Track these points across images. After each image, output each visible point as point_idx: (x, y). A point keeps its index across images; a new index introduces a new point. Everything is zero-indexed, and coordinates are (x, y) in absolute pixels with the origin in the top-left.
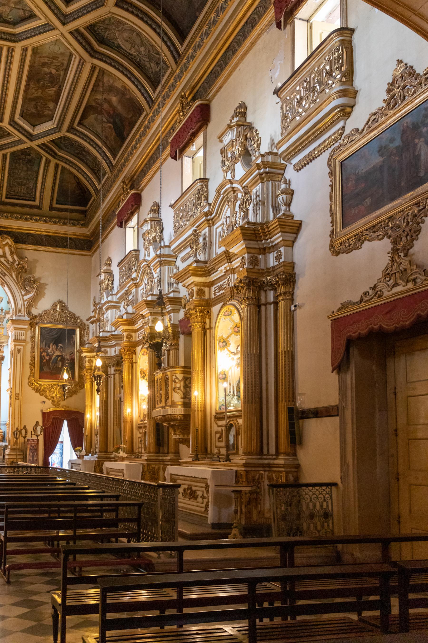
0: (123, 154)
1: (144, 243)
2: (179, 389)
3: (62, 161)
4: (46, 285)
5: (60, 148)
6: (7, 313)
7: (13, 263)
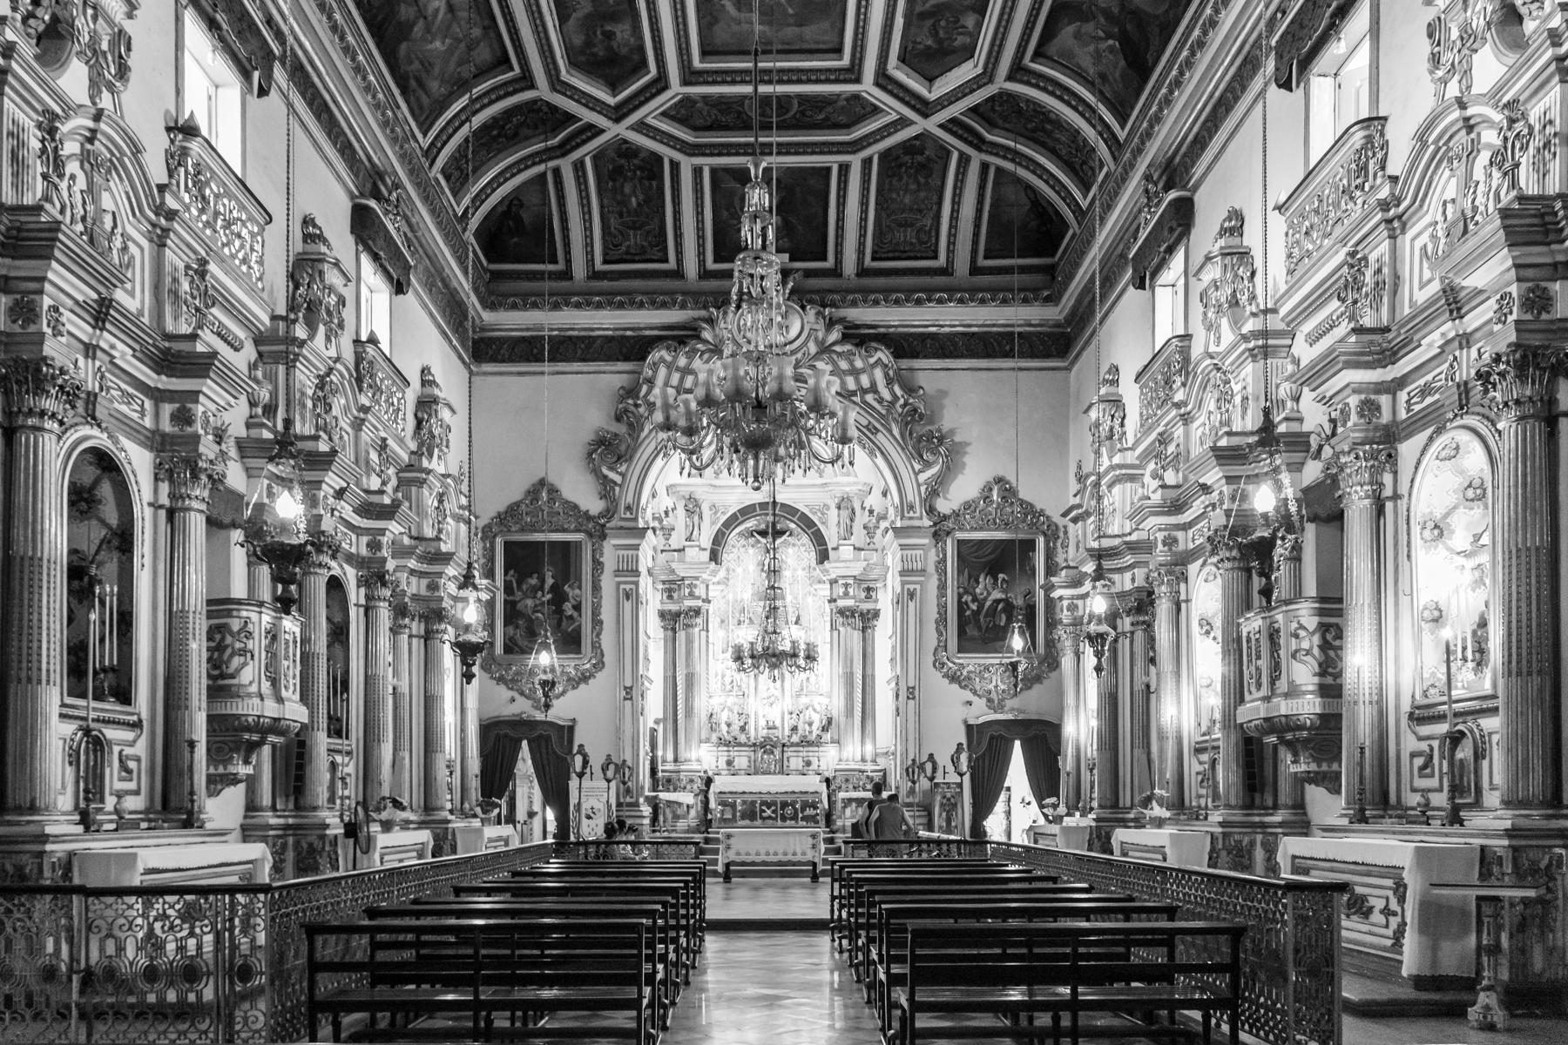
0: (1147, 106)
1: (1205, 314)
2: (1308, 652)
3: (997, 155)
4: (968, 444)
5: (991, 124)
6: (884, 517)
7: (892, 403)
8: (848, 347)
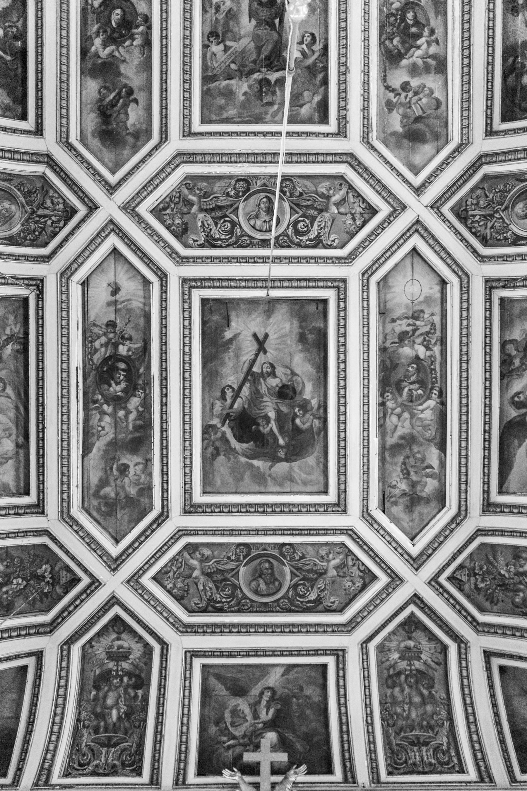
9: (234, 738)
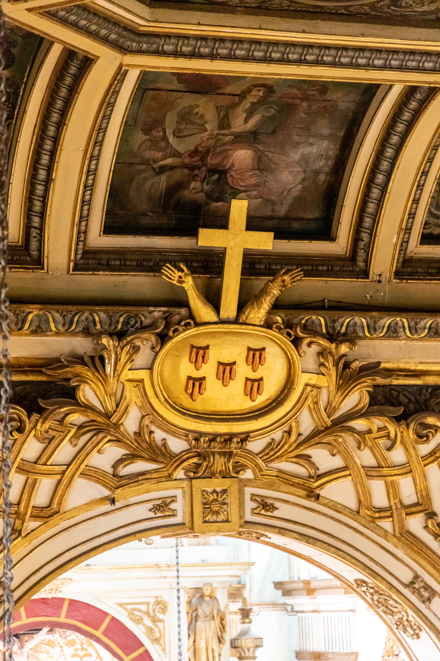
8: (377, 422)
9: (176, 154)
